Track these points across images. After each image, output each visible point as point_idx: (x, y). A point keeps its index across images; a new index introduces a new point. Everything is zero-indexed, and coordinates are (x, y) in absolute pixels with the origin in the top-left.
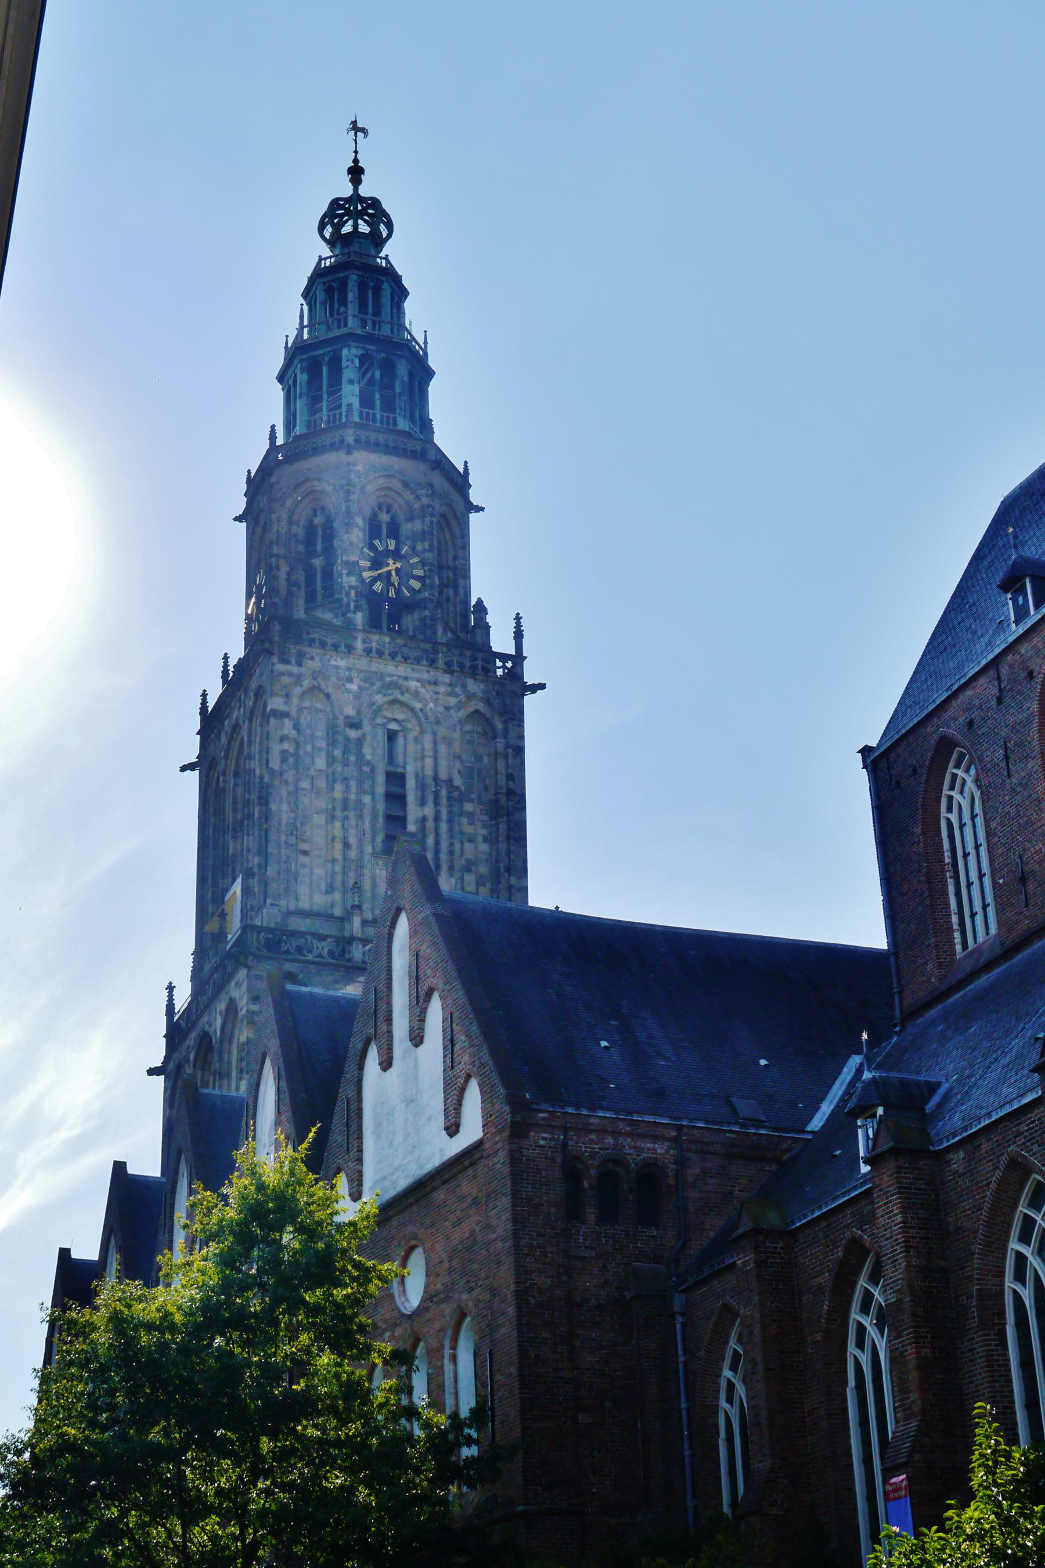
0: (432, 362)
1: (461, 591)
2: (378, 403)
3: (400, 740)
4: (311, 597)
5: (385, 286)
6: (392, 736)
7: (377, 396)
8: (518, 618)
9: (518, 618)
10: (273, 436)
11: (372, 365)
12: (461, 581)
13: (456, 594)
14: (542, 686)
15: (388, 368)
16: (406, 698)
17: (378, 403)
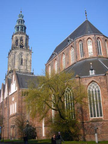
4: (16, 45)
15: (23, 28)
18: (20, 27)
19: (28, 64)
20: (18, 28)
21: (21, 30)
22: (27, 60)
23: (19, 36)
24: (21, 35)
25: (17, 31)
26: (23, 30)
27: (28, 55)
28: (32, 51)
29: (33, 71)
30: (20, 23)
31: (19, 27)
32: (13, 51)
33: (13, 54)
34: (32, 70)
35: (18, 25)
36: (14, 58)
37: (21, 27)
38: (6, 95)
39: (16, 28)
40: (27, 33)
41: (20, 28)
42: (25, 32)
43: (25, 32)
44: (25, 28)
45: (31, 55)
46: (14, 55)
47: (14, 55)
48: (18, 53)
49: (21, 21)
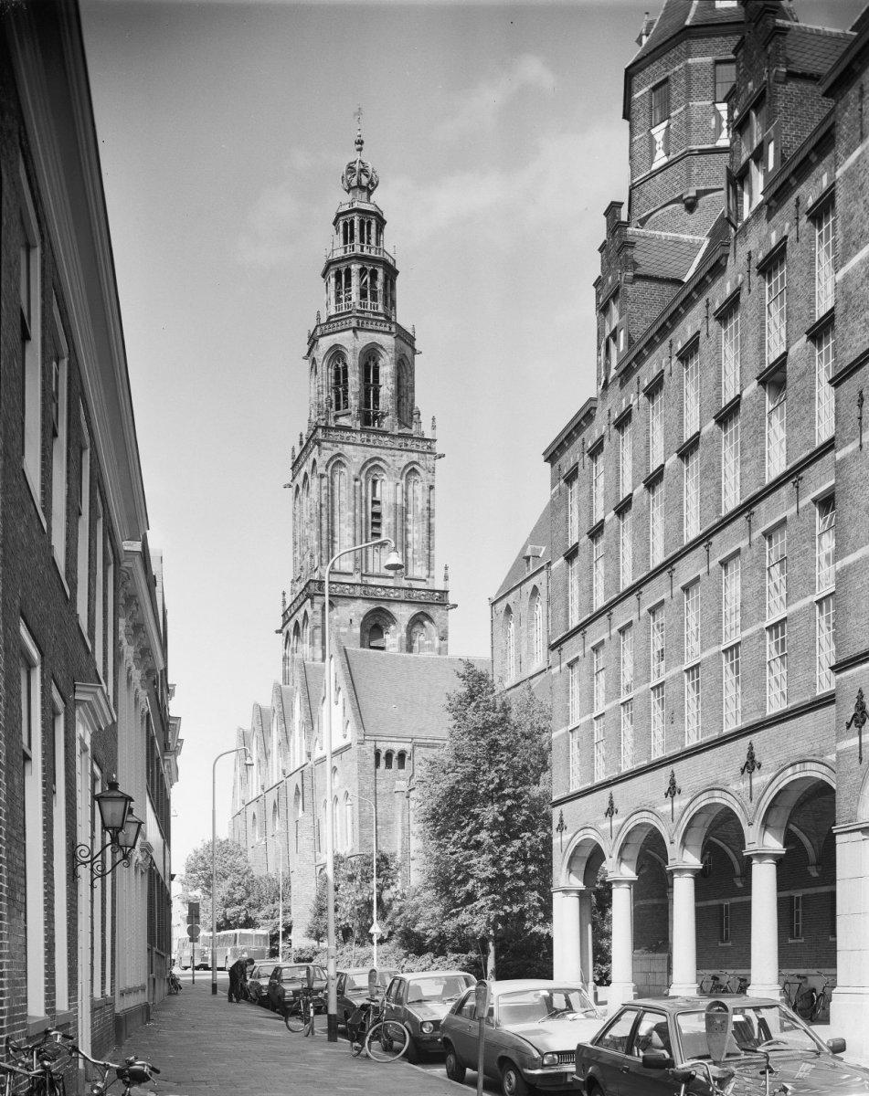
0: (398, 267)
1: (410, 399)
2: (369, 296)
3: (379, 483)
4: (338, 408)
5: (374, 222)
6: (375, 482)
7: (369, 293)
8: (434, 419)
9: (434, 419)
10: (319, 319)
11: (366, 273)
12: (410, 394)
13: (407, 400)
14: (444, 455)
15: (374, 275)
16: (381, 464)
17: (369, 296)
18: (355, 268)
19: (416, 534)
20: (343, 278)
21: (363, 295)
22: (405, 511)
23: (352, 343)
24: (365, 338)
25: (338, 300)
26: (374, 298)
27: (413, 478)
28: (438, 448)
29: (446, 578)
30: (357, 239)
31: (348, 272)
32: (321, 456)
33: (321, 470)
34: (438, 572)
35: (340, 254)
36: (331, 496)
37: (362, 272)
38: (297, 758)
39: (333, 280)
40: (404, 317)
41: (355, 280)
42: (393, 303)
43: (390, 302)
44: (391, 273)
45: (432, 471)
46: (325, 481)
47: (325, 481)
48: (351, 470)
49: (362, 223)
